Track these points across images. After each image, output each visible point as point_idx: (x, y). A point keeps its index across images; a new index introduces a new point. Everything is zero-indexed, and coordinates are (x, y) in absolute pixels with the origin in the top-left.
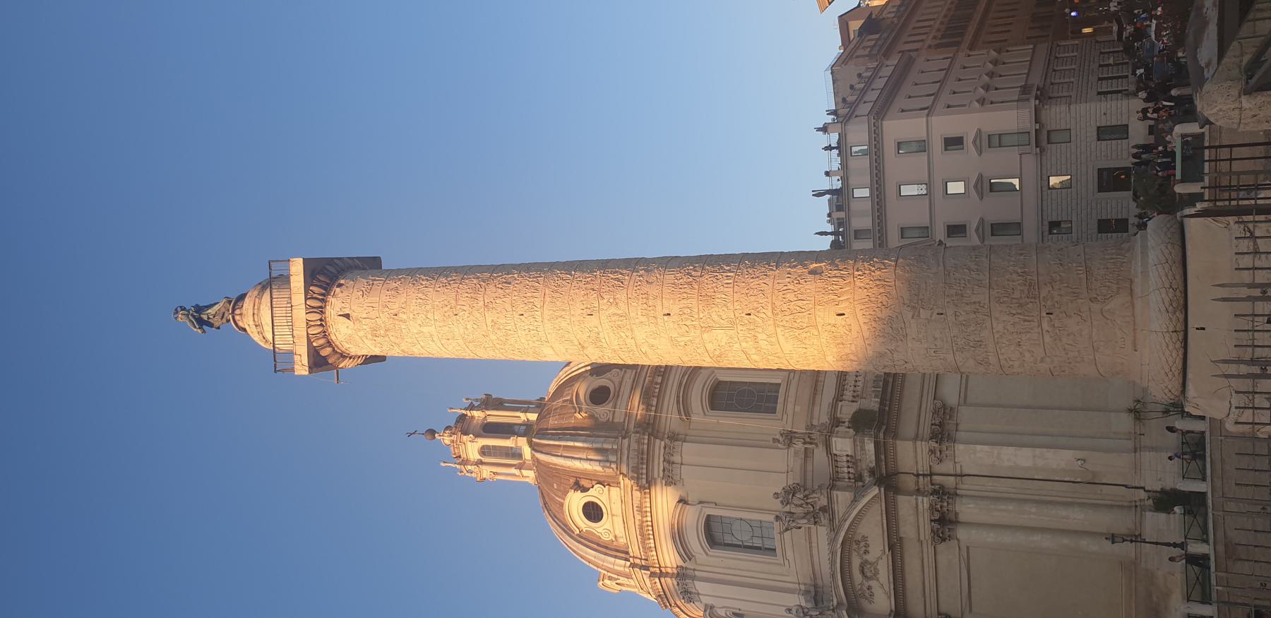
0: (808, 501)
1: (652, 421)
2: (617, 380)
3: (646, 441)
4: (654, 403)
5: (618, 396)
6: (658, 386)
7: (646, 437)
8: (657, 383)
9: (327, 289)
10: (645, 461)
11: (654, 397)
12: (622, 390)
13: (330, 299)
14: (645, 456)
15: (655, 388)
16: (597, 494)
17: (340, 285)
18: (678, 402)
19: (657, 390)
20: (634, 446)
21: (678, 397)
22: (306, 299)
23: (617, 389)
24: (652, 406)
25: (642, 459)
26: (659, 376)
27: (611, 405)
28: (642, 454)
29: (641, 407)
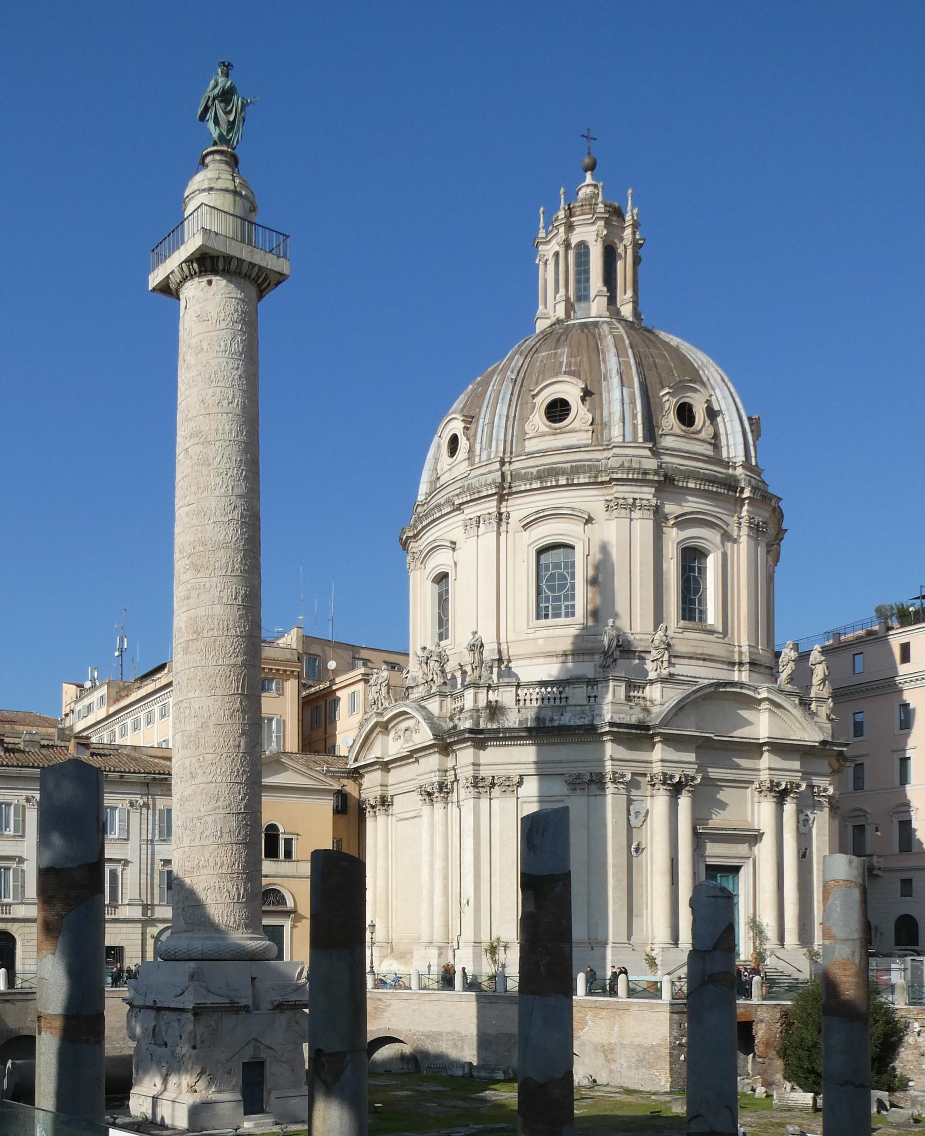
0: (435, 675)
1: (514, 490)
2: (576, 425)
3: (490, 492)
4: (534, 486)
5: (555, 434)
6: (554, 484)
7: (494, 491)
8: (557, 481)
9: (203, 272)
10: (473, 497)
11: (541, 482)
12: (564, 435)
13: (196, 279)
14: (476, 496)
15: (551, 481)
16: (463, 443)
17: (210, 283)
18: (537, 512)
19: (549, 484)
20: (490, 478)
21: (543, 510)
22: (185, 262)
23: (564, 430)
24: (531, 484)
25: (474, 493)
26: (567, 479)
27: (547, 429)
28: (479, 492)
29: (534, 470)
